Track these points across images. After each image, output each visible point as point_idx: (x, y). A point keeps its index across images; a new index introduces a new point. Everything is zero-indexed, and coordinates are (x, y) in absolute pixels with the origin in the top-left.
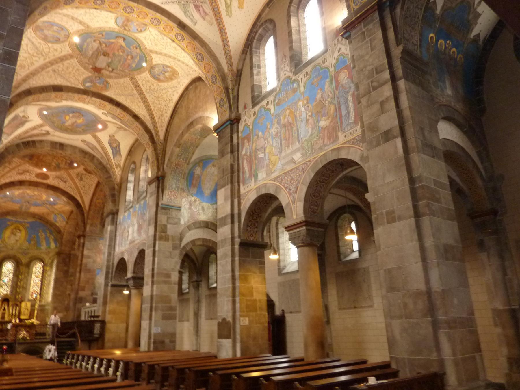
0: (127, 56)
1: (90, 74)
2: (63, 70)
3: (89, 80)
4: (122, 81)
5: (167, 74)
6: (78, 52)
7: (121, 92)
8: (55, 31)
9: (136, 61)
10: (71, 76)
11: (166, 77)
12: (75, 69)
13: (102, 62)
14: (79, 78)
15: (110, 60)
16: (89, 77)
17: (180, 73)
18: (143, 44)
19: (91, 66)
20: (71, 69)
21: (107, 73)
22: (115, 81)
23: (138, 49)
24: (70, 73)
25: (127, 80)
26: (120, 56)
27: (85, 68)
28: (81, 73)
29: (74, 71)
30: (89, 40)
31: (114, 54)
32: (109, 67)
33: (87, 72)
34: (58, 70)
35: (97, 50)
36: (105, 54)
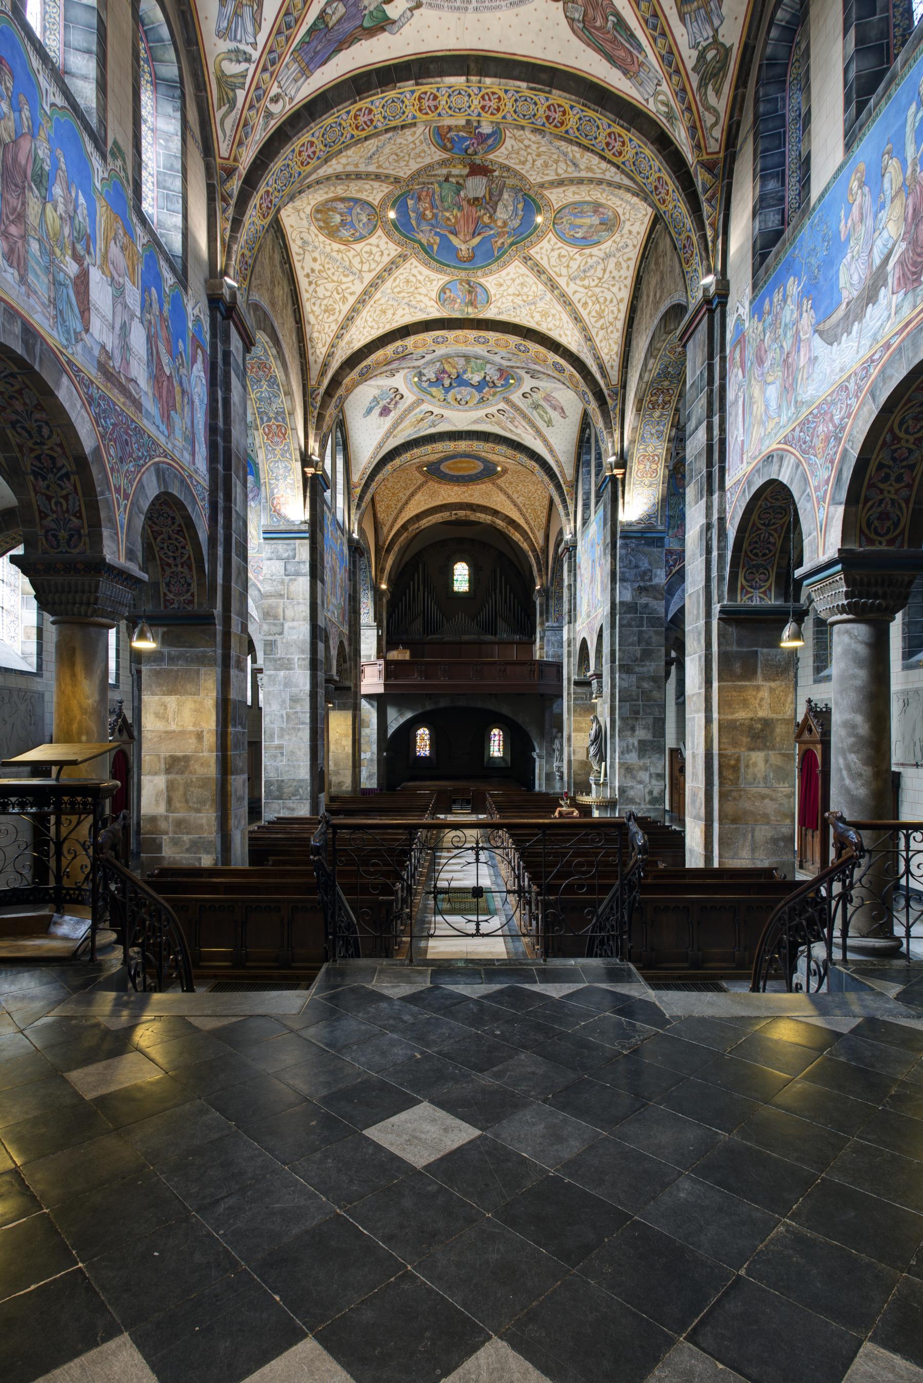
0: (435, 216)
1: (491, 157)
2: (556, 162)
3: (490, 142)
4: (414, 166)
5: (338, 219)
6: (531, 193)
7: (399, 141)
8: (580, 227)
9: (412, 215)
10: (534, 147)
11: (334, 209)
12: (528, 165)
13: (477, 187)
14: (513, 142)
15: (462, 194)
16: (492, 148)
17: (322, 238)
18: (426, 264)
19: (496, 174)
20: (539, 163)
21: (455, 171)
22: (428, 160)
23: (424, 241)
24: (539, 155)
25: (404, 172)
26: (447, 210)
27: (508, 169)
28: (514, 156)
29: (529, 158)
30: (516, 223)
31: (460, 208)
32: (458, 183)
33: (500, 160)
34: (568, 165)
35: (496, 204)
36: (475, 201)
